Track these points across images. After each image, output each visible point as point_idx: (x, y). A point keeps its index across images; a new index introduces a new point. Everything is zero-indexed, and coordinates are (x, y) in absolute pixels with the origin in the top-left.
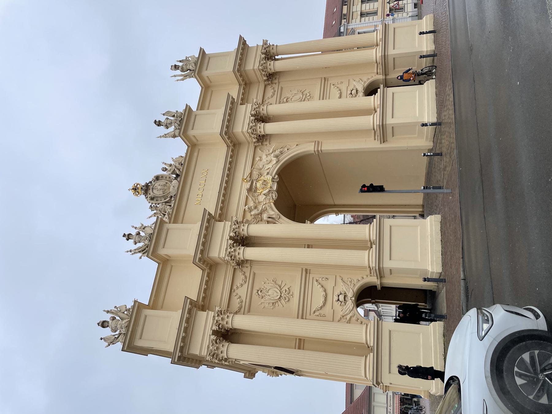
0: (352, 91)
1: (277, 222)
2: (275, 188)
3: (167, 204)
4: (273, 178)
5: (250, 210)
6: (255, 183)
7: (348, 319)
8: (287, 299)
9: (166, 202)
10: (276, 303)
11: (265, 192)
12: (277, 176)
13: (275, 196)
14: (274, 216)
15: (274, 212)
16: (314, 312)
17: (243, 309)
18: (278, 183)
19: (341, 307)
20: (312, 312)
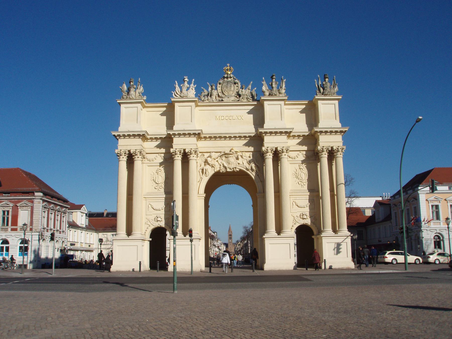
0: (306, 215)
1: (203, 175)
2: (228, 170)
3: (217, 95)
4: (236, 168)
5: (210, 157)
6: (231, 157)
7: (148, 223)
8: (156, 188)
9: (218, 95)
10: (154, 181)
11: (226, 165)
12: (238, 170)
13: (223, 170)
14: (207, 172)
15: (211, 172)
16: (149, 204)
17: (150, 162)
18: (234, 171)
19: (154, 219)
20: (150, 203)
